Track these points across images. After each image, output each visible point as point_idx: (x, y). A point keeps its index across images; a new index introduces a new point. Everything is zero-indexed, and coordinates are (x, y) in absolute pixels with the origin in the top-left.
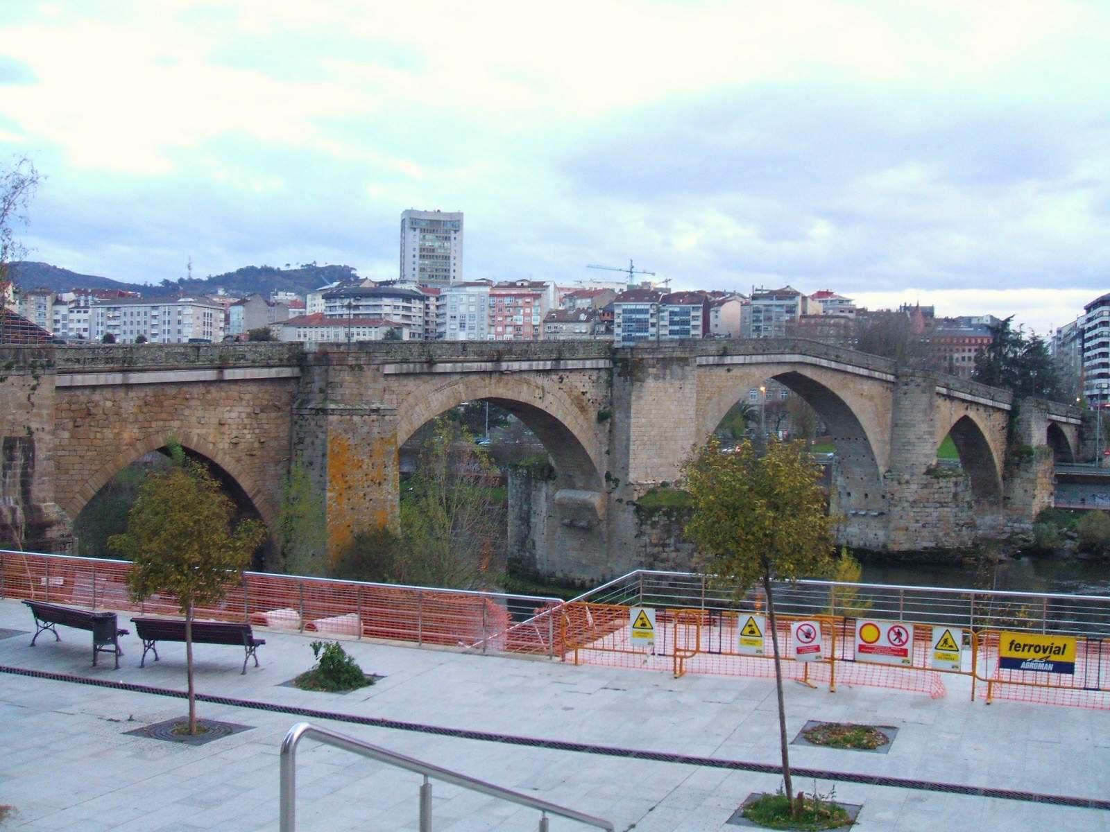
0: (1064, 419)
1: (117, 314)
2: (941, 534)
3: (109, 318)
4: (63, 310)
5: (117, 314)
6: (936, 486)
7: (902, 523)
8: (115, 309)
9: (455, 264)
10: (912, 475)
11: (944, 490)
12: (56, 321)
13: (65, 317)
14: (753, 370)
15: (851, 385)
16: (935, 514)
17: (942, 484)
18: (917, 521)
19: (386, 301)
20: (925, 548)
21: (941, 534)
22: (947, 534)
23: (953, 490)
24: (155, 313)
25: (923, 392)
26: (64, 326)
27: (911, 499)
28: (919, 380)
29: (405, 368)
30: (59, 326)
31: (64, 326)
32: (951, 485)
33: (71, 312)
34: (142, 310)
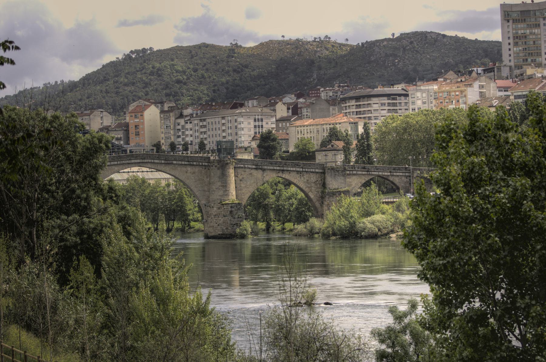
0: (389, 174)
1: (205, 123)
2: (224, 228)
3: (201, 127)
4: (182, 121)
5: (205, 123)
6: (223, 208)
7: (212, 224)
8: (204, 120)
9: (510, 55)
10: (214, 204)
11: (226, 210)
12: (179, 130)
13: (183, 127)
14: (113, 167)
15: (179, 169)
16: (222, 220)
17: (225, 207)
18: (216, 223)
19: (375, 100)
20: (219, 234)
21: (224, 228)
22: (227, 229)
23: (230, 209)
24: (223, 121)
25: (218, 169)
26: (183, 133)
27: (214, 214)
28: (216, 164)
29: (166, 162)
30: (180, 133)
31: (183, 133)
32: (229, 207)
33: (187, 123)
34: (217, 120)
